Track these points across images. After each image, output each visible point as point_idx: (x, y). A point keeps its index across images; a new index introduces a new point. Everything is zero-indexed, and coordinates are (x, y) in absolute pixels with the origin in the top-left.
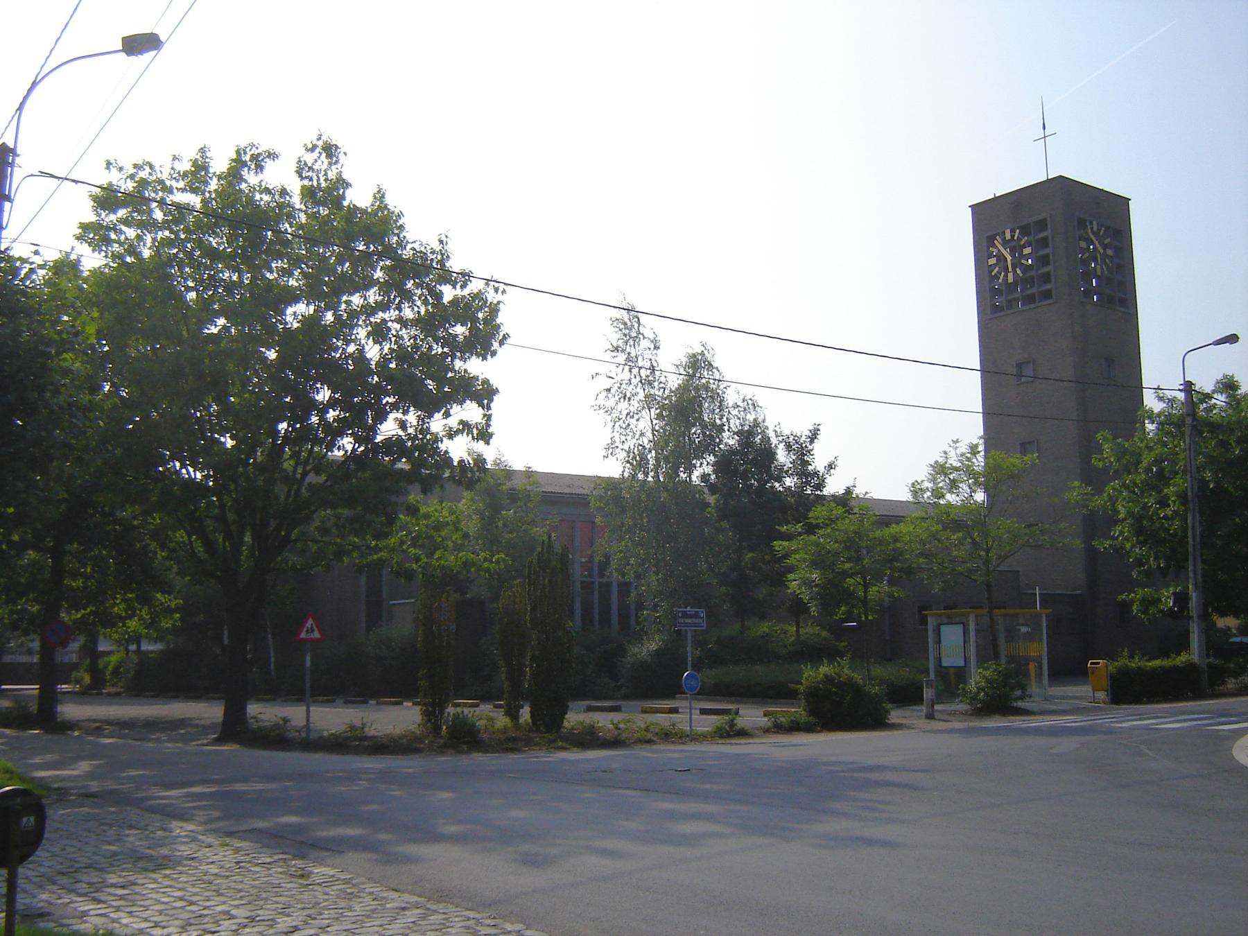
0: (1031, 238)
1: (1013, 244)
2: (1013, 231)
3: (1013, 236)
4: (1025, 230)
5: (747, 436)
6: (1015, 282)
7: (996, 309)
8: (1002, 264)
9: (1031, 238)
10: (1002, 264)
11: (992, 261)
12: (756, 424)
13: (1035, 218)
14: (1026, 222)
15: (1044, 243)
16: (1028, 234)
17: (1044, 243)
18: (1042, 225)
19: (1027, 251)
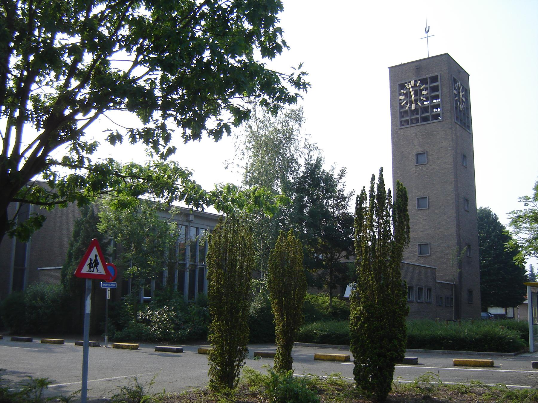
0: (428, 86)
1: (416, 89)
2: (416, 81)
3: (416, 85)
4: (424, 81)
5: (314, 169)
6: (417, 110)
7: (401, 124)
8: (408, 100)
9: (428, 86)
10: (408, 100)
11: (402, 97)
12: (319, 161)
13: (430, 75)
14: (424, 77)
15: (435, 89)
16: (426, 84)
17: (435, 89)
18: (434, 79)
19: (424, 93)
